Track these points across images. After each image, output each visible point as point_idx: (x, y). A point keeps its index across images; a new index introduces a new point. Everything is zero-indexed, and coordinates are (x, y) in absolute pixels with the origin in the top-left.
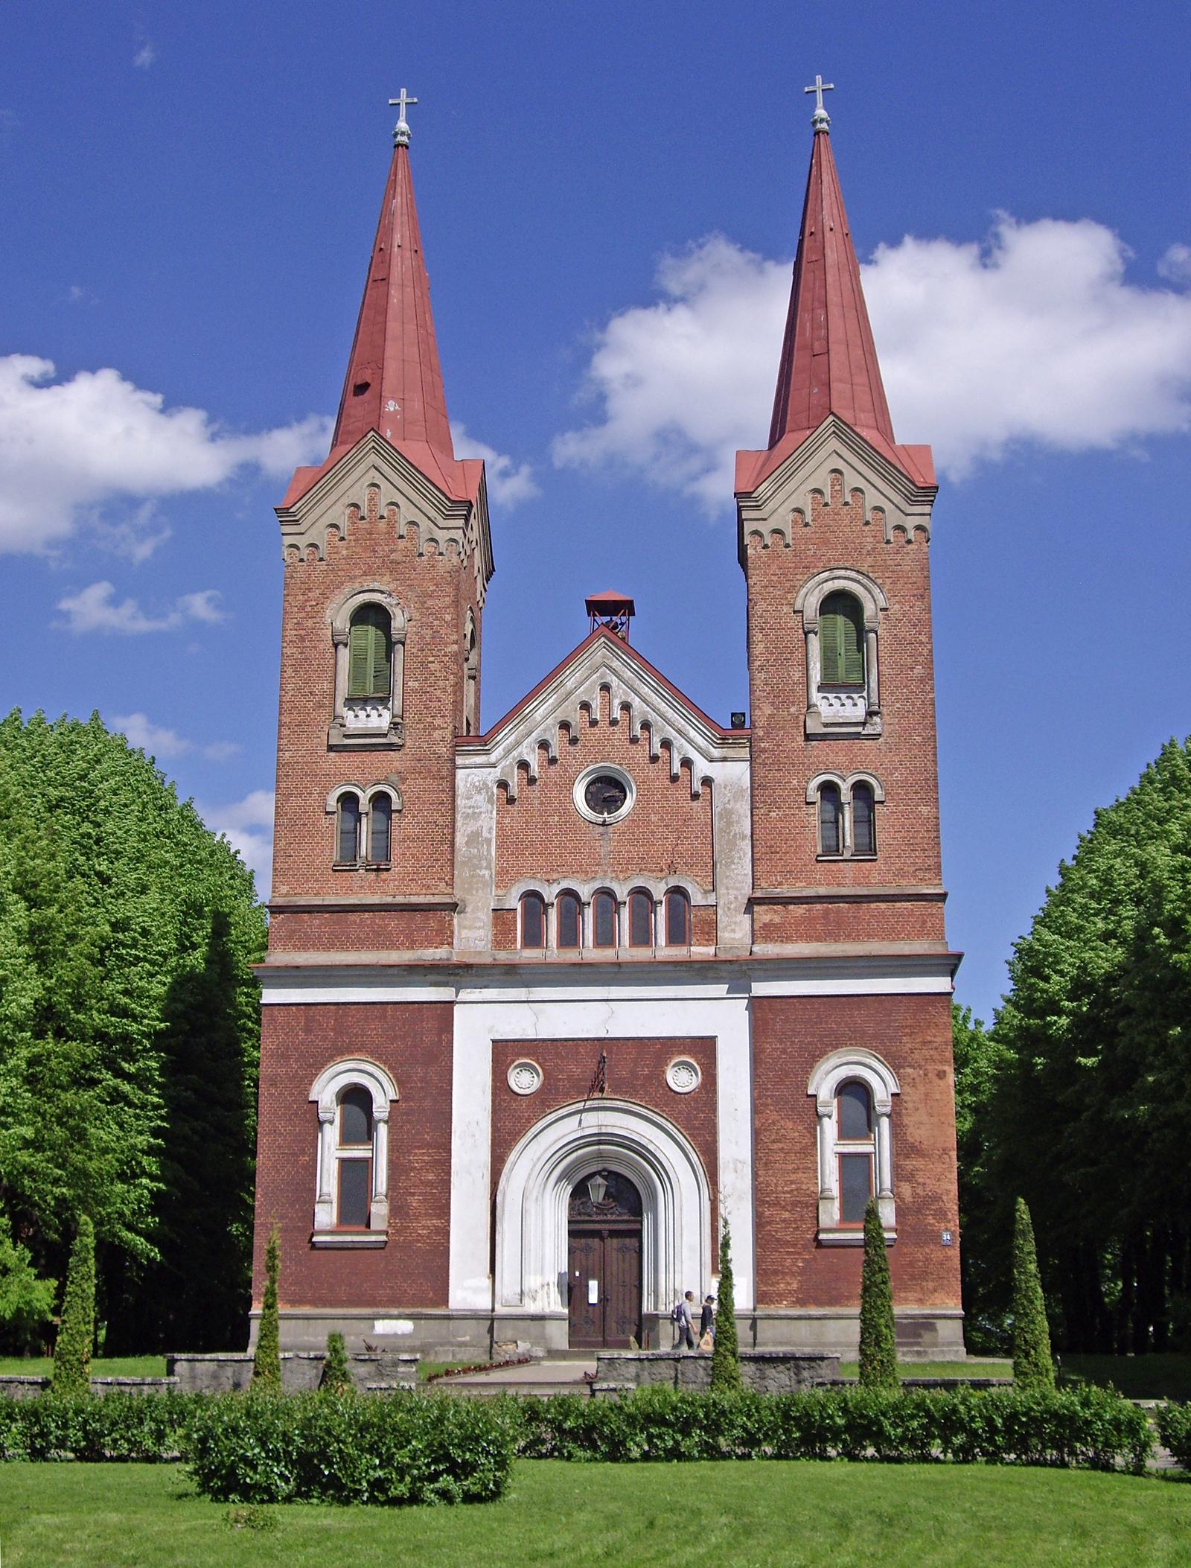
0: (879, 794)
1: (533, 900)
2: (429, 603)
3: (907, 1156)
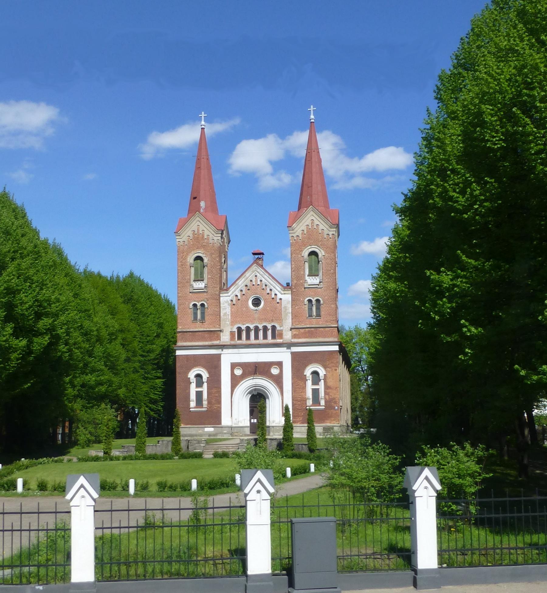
0: (322, 302)
1: (240, 330)
2: (213, 256)
3: (327, 389)
